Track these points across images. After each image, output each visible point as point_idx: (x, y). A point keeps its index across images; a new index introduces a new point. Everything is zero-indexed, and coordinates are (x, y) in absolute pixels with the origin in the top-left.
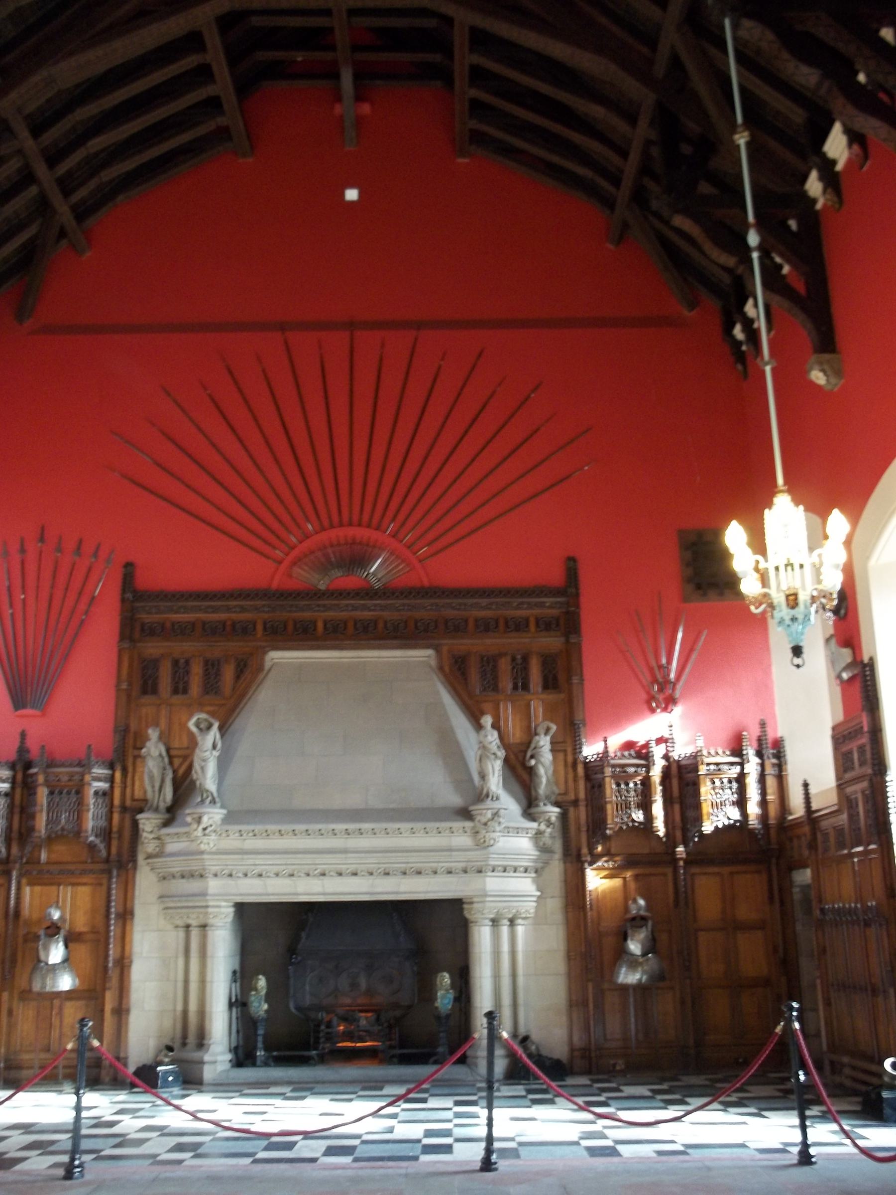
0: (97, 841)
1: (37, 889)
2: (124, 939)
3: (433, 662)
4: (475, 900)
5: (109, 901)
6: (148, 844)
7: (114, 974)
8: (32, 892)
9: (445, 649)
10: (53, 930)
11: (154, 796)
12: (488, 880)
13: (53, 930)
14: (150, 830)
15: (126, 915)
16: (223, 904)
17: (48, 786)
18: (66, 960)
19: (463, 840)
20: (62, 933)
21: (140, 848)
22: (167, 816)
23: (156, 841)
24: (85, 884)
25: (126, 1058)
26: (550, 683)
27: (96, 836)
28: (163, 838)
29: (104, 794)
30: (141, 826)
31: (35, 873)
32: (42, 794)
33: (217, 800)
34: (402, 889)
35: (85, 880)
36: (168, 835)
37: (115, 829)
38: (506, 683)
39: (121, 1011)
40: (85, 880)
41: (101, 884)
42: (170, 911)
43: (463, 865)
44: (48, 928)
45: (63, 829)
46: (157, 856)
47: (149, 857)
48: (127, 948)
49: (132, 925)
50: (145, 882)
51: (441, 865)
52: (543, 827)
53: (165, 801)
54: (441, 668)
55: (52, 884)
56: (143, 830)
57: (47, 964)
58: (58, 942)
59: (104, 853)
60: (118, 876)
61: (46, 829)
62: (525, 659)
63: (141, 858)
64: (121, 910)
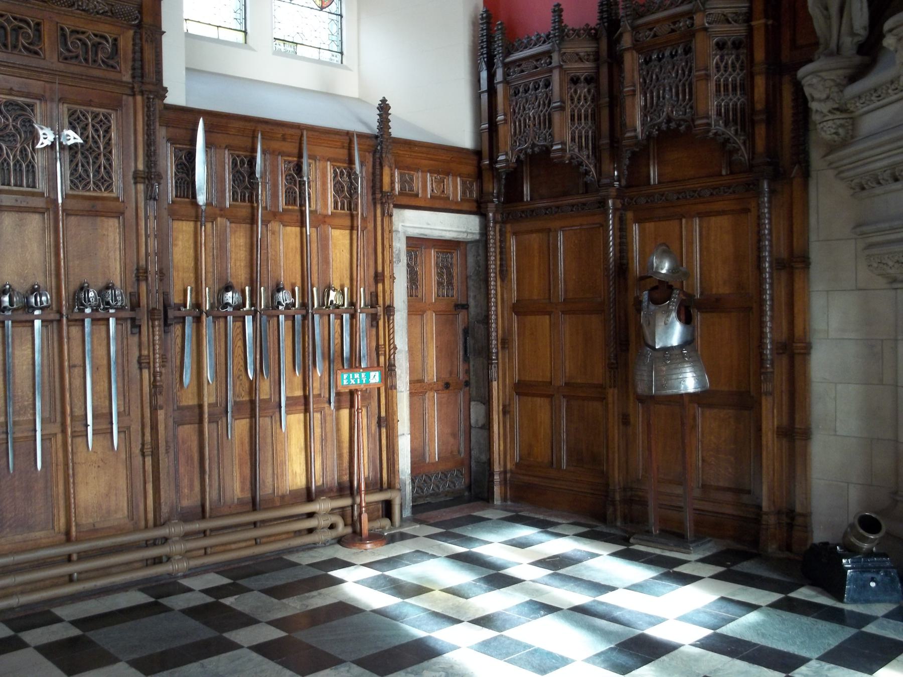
0: (731, 132)
1: (650, 226)
2: (793, 307)
5: (760, 238)
6: (825, 127)
7: (777, 369)
8: (642, 232)
10: (661, 291)
11: (830, 28)
13: (661, 291)
14: (824, 96)
15: (795, 263)
17: (639, 51)
18: (687, 343)
20: (676, 297)
21: (813, 137)
22: (858, 59)
23: (838, 115)
24: (722, 213)
25: (807, 515)
27: (726, 124)
28: (851, 107)
29: (737, 45)
30: (807, 91)
31: (643, 200)
32: (631, 62)
35: (717, 206)
37: (759, 106)
39: (796, 433)
40: (717, 206)
41: (746, 211)
42: (875, 251)
44: (655, 288)
46: (844, 144)
47: (832, 148)
48: (799, 321)
49: (807, 279)
50: (828, 204)
53: (853, 34)
55: (668, 218)
56: (813, 99)
57: (653, 348)
58: (668, 312)
59: (744, 155)
60: (772, 192)
61: (643, 125)
63: (815, 156)
64: (784, 254)
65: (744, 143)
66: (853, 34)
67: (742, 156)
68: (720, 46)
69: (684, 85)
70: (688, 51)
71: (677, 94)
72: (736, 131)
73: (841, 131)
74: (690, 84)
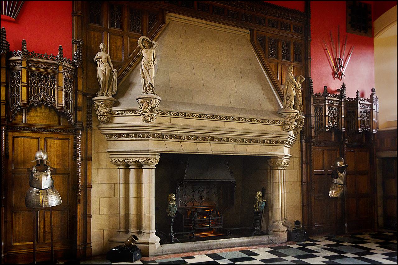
3: (249, 38)
4: (279, 157)
9: (255, 32)
12: (284, 147)
16: (157, 154)
19: (277, 128)
26: (297, 59)
33: (155, 93)
34: (248, 151)
36: (117, 111)
38: (281, 53)
43: (278, 139)
45: (43, 101)
51: (268, 138)
52: (299, 125)
53: (112, 91)
54: (252, 41)
62: (289, 44)
63: (94, 125)
65: (72, 116)
66: (112, 91)
67: (71, 120)
68: (66, 80)
69: (51, 90)
70: (53, 77)
71: (48, 92)
72: (70, 111)
73: (108, 119)
74: (54, 90)
